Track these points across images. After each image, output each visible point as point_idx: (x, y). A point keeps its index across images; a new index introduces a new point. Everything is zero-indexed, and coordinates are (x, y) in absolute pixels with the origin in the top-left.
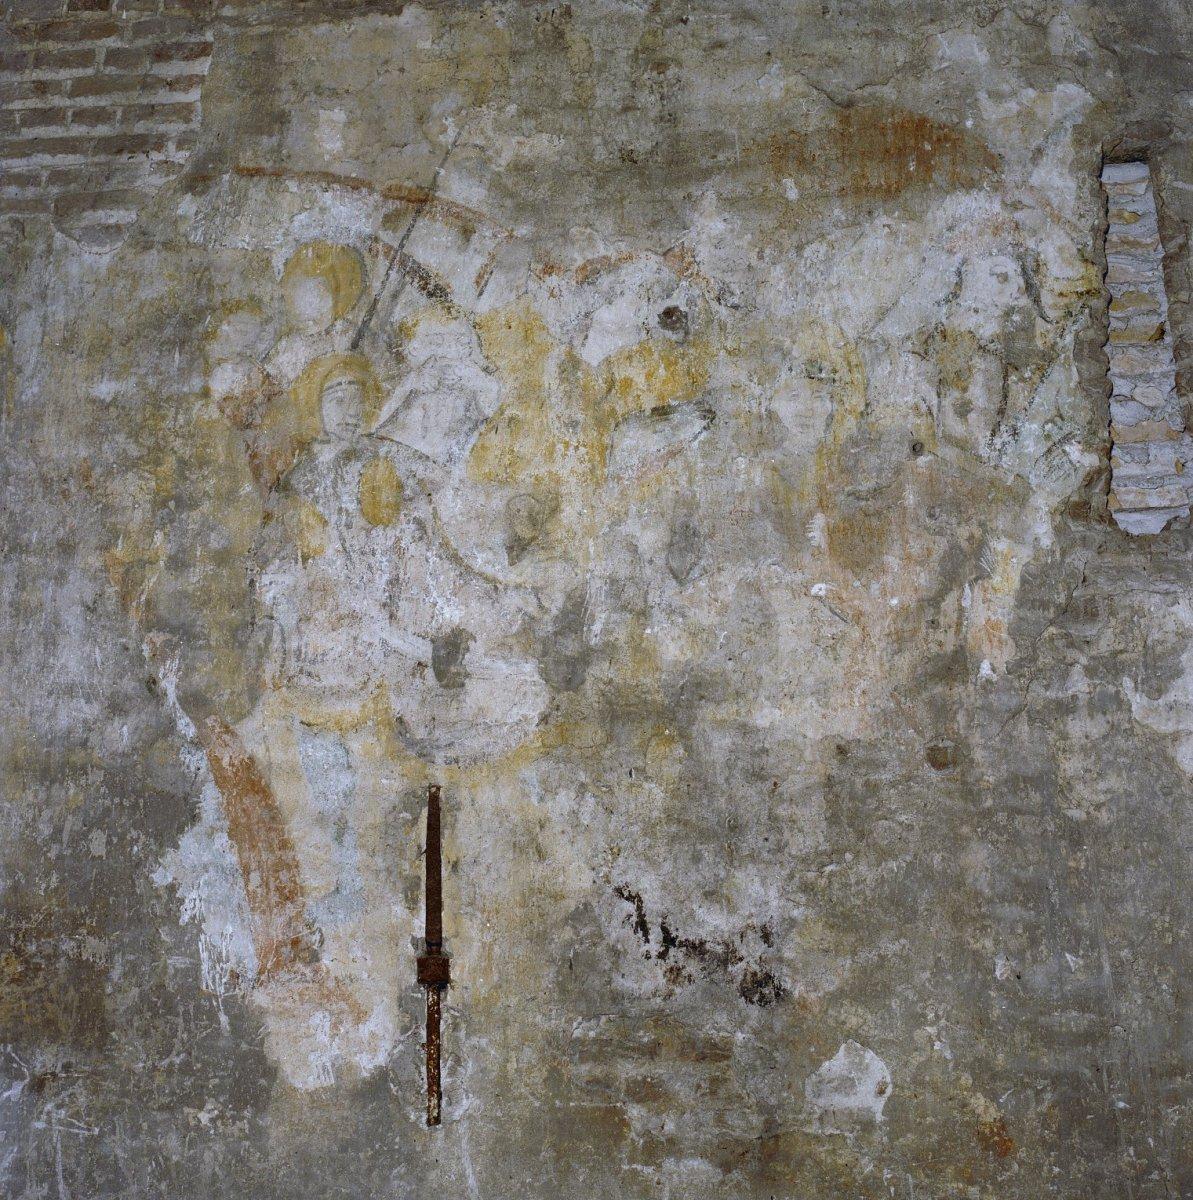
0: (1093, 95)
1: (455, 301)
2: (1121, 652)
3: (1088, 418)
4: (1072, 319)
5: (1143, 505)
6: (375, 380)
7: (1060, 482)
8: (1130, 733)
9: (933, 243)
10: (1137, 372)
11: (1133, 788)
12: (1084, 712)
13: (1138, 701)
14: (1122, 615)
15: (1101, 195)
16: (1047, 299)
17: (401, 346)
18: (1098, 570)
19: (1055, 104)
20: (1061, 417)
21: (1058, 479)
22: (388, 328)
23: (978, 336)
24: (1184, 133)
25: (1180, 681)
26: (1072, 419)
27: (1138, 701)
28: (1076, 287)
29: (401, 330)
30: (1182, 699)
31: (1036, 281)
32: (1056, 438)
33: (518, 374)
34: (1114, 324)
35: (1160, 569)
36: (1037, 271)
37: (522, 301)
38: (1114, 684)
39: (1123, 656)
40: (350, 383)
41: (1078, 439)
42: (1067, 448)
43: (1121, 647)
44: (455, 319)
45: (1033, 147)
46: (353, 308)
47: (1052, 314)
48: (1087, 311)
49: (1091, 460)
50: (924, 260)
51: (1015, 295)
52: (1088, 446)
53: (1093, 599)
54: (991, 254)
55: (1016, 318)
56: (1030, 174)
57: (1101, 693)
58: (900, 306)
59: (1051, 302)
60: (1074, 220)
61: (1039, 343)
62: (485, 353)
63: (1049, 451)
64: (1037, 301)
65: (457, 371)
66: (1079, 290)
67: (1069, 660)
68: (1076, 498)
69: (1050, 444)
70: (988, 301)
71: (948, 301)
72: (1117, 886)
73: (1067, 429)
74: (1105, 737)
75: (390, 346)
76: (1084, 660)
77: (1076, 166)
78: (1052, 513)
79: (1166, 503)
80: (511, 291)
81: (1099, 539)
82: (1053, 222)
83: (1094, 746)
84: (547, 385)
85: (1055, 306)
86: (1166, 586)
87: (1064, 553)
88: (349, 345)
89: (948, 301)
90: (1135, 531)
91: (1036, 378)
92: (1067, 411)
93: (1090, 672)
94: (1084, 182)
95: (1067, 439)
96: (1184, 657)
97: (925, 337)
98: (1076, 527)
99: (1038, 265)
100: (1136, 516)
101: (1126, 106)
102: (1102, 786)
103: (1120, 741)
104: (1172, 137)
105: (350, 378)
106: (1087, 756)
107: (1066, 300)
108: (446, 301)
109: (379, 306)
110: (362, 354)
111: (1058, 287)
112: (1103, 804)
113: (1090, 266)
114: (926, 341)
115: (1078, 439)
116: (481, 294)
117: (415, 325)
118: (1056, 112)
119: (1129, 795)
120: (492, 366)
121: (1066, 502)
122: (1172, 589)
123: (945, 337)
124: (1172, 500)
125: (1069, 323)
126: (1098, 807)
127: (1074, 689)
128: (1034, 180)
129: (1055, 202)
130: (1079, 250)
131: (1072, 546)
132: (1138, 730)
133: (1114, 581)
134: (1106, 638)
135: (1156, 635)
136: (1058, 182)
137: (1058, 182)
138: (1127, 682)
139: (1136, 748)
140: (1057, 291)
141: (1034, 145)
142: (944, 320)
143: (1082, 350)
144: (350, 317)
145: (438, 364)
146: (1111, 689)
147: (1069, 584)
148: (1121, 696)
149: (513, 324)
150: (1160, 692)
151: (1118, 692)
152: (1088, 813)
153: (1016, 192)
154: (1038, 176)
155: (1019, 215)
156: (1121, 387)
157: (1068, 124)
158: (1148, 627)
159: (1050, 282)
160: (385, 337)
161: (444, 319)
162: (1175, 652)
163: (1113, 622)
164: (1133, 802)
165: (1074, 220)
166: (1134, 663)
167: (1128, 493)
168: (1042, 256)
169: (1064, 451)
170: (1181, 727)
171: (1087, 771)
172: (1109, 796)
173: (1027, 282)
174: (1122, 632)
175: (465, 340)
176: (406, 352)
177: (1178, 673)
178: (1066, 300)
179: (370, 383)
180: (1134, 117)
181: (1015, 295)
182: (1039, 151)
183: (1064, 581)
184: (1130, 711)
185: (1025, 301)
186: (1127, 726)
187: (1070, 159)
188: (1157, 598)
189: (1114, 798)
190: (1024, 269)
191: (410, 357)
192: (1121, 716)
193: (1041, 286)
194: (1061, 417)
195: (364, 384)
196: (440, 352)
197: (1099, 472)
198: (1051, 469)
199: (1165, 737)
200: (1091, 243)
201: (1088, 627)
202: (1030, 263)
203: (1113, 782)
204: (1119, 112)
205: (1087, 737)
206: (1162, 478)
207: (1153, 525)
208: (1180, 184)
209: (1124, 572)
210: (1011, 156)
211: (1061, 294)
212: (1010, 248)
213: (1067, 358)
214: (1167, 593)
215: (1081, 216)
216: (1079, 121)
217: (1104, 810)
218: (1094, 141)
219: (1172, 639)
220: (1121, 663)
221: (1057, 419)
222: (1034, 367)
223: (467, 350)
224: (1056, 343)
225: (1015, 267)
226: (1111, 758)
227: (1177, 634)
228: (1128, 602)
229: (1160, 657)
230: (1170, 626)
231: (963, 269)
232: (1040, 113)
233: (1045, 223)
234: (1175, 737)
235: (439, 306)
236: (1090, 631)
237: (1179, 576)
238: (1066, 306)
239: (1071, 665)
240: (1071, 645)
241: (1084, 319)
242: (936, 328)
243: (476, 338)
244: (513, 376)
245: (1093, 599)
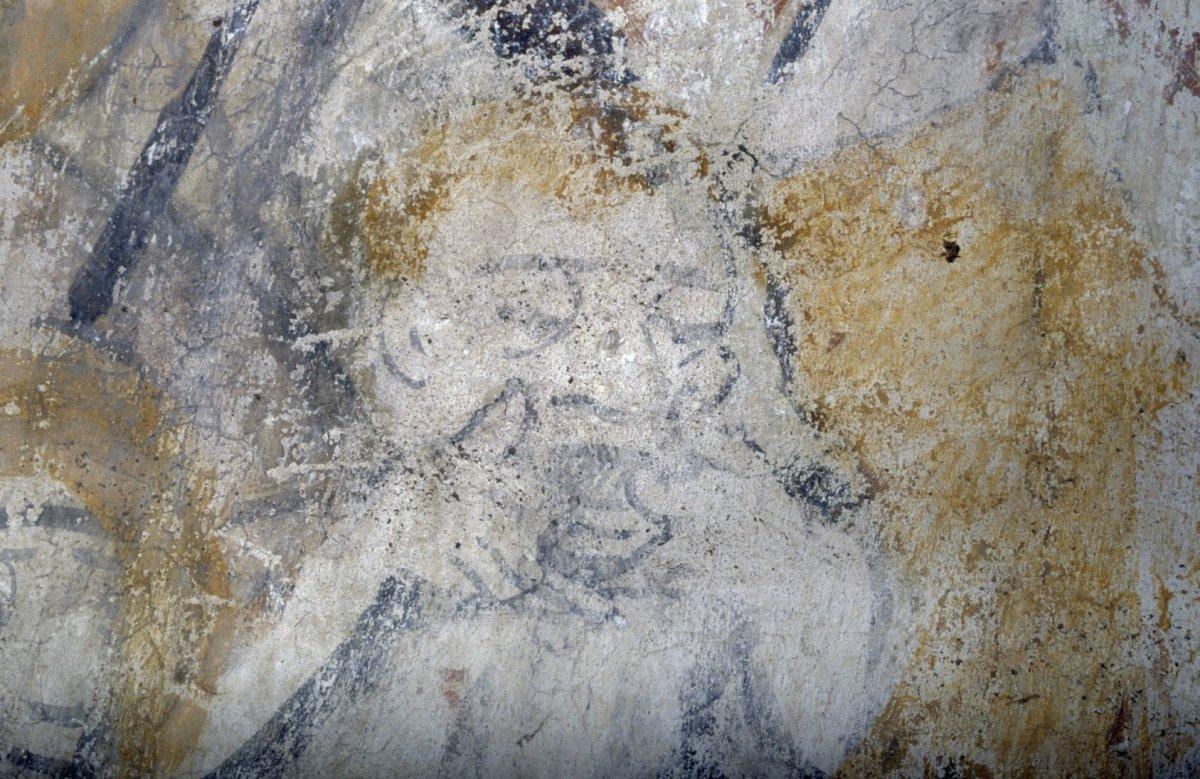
1: (652, 78)
6: (189, 507)
17: (339, 320)
22: (276, 210)
29: (345, 230)
33: (986, 527)
37: (1020, 104)
40: (50, 516)
44: (650, 181)
46: (91, 90)
62: (805, 389)
65: (643, 480)
75: (279, 319)
80: (962, 39)
84: (1149, 604)
88: (55, 295)
105: (52, 488)
108: (600, 75)
109: (233, 85)
110: (127, 355)
116: (793, 48)
117: (422, 205)
120: (843, 470)
144: (71, 137)
145: (544, 437)
149: (963, 234)
160: (257, 261)
161: (586, 177)
175: (701, 307)
176: (369, 357)
179: (164, 523)
191: (387, 387)
195: (123, 527)
196: (555, 369)
223: (708, 372)
235: (562, 103)
243: (751, 297)
244: (962, 538)
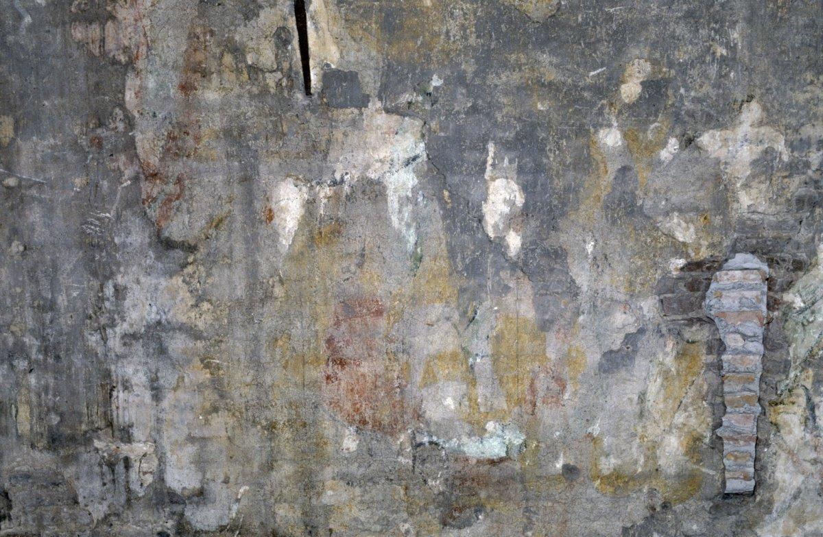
0: (756, 534)
2: (786, 177)
3: (787, 324)
4: (789, 387)
5: (745, 271)
7: (809, 284)
8: (787, 127)
10: (739, 356)
11: (790, 93)
12: (813, 141)
13: (780, 146)
14: (783, 200)
15: (760, 466)
16: (802, 401)
18: (793, 228)
19: (781, 529)
20: (803, 325)
21: (811, 285)
24: (703, 506)
25: (754, 157)
26: (797, 324)
27: (780, 146)
30: (753, 146)
31: (808, 413)
32: (808, 311)
34: (755, 386)
35: (755, 227)
36: (807, 419)
38: (794, 156)
39: (785, 174)
41: (795, 311)
42: (802, 305)
43: (786, 180)
45: (799, 500)
47: (801, 391)
48: (779, 392)
49: (788, 297)
52: (790, 306)
53: (798, 210)
56: (803, 482)
57: (803, 151)
59: (801, 399)
60: (780, 452)
61: (811, 372)
63: (813, 304)
64: (809, 399)
66: (782, 406)
67: (819, 173)
68: (801, 273)
69: (812, 308)
72: (807, 35)
73: (801, 317)
74: (803, 125)
76: (810, 172)
77: (772, 487)
78: (817, 264)
79: (730, 273)
81: (788, 248)
82: (793, 451)
83: (810, 120)
85: (798, 396)
86: (753, 216)
87: (813, 239)
90: (749, 256)
91: (816, 350)
92: (800, 329)
93: (807, 165)
94: (770, 476)
95: (802, 311)
96: (748, 173)
98: (802, 256)
99: (805, 423)
100: (746, 266)
101: (737, 526)
102: (808, 95)
103: (794, 122)
104: (711, 504)
106: (815, 114)
107: (791, 399)
111: (795, 408)
112: (809, 84)
113: (774, 421)
115: (795, 311)
118: (781, 521)
119: (791, 89)
121: (808, 270)
122: (749, 215)
124: (727, 274)
125: (791, 385)
126: (812, 82)
127: (819, 155)
128: (801, 478)
129: (790, 464)
130: (779, 432)
131: (807, 243)
132: (782, 129)
133: (784, 222)
134: (795, 185)
135: (763, 187)
136: (787, 477)
137: (787, 477)
138: (785, 158)
139: (785, 118)
140: (796, 405)
141: (798, 502)
143: (785, 367)
146: (796, 154)
147: (813, 219)
148: (790, 149)
150: (766, 152)
151: (792, 152)
152: (818, 79)
153: (813, 471)
154: (798, 481)
155: (813, 455)
156: (757, 347)
157: (775, 515)
158: (767, 191)
159: (800, 411)
162: (753, 176)
163: (789, 195)
164: (790, 85)
165: (780, 452)
166: (779, 170)
167: (753, 280)
168: (802, 428)
169: (804, 303)
170: (756, 130)
171: (816, 105)
172: (805, 89)
174: (784, 189)
177: (754, 163)
178: (791, 399)
180: (733, 518)
182: (795, 497)
183: (815, 222)
184: (785, 140)
185: (816, 400)
186: (788, 131)
187: (776, 492)
188: (760, 209)
189: (802, 88)
190: (815, 420)
192: (791, 138)
193: (805, 409)
194: (803, 325)
197: (783, 290)
198: (814, 292)
199: (767, 124)
200: (772, 436)
201: (804, 193)
202: (810, 424)
203: (801, 97)
204: (742, 522)
205: (813, 125)
206: (734, 288)
207: (740, 259)
208: (712, 472)
209: (779, 226)
210: (813, 494)
211: (793, 403)
213: (795, 362)
214: (753, 212)
215: (775, 454)
216: (767, 517)
217: (809, 81)
218: (761, 503)
219: (754, 184)
220: (786, 170)
221: (805, 323)
222: (816, 357)
224: (801, 372)
226: (801, 112)
227: (750, 187)
228: (778, 207)
229: (763, 173)
230: (754, 192)
232: (791, 523)
233: (798, 450)
234: (761, 123)
236: (802, 191)
237: (744, 223)
238: (791, 395)
239: (817, 170)
240: (816, 182)
241: (782, 387)
245: (798, 210)
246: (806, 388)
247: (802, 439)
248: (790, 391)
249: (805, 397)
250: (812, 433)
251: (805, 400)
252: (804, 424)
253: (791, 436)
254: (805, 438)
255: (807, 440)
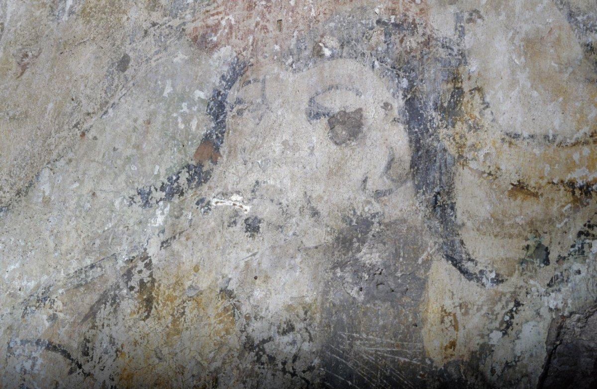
4: (547, 272)
9: (156, 16)
23: (246, 309)
28: (571, 166)
50: (124, 63)
51: (377, 182)
54: (318, 53)
55: (370, 256)
58: (36, 198)
59: (484, 211)
70: (294, 195)
71: (172, 191)
89: (172, 191)
97: (92, 298)
99: (458, 92)
107: (533, 209)
114: (92, 313)
123: (149, 302)
125: (537, 285)
142: (153, 250)
168: (474, 66)
173: (416, 144)
178: (533, 209)
181: (377, 182)
190: (410, 104)
211: (520, 188)
212: (378, 37)
225: (387, 96)
231: (233, 95)
238: (534, 228)
242: (128, 274)
246: (456, 263)
247: (475, 15)
248: (542, 253)
249: (460, 217)
250: (426, 44)
251: (461, 202)
252: (466, 86)
253: (526, 27)
254: (458, 18)
255: (452, 9)
